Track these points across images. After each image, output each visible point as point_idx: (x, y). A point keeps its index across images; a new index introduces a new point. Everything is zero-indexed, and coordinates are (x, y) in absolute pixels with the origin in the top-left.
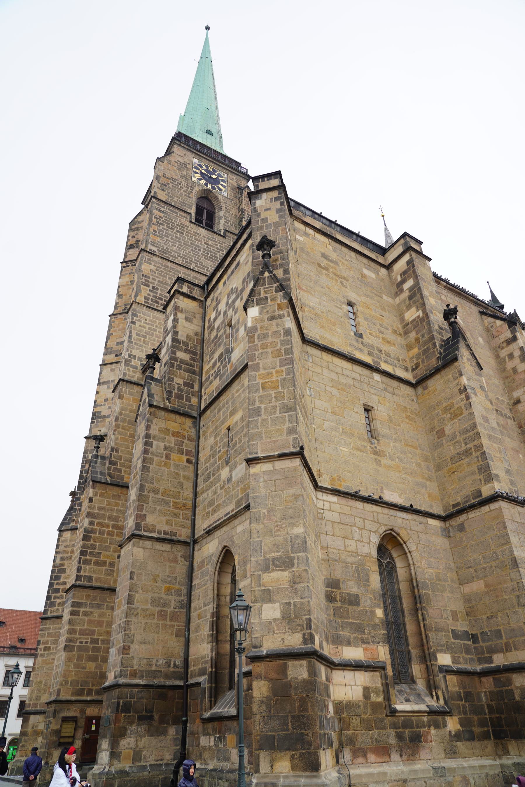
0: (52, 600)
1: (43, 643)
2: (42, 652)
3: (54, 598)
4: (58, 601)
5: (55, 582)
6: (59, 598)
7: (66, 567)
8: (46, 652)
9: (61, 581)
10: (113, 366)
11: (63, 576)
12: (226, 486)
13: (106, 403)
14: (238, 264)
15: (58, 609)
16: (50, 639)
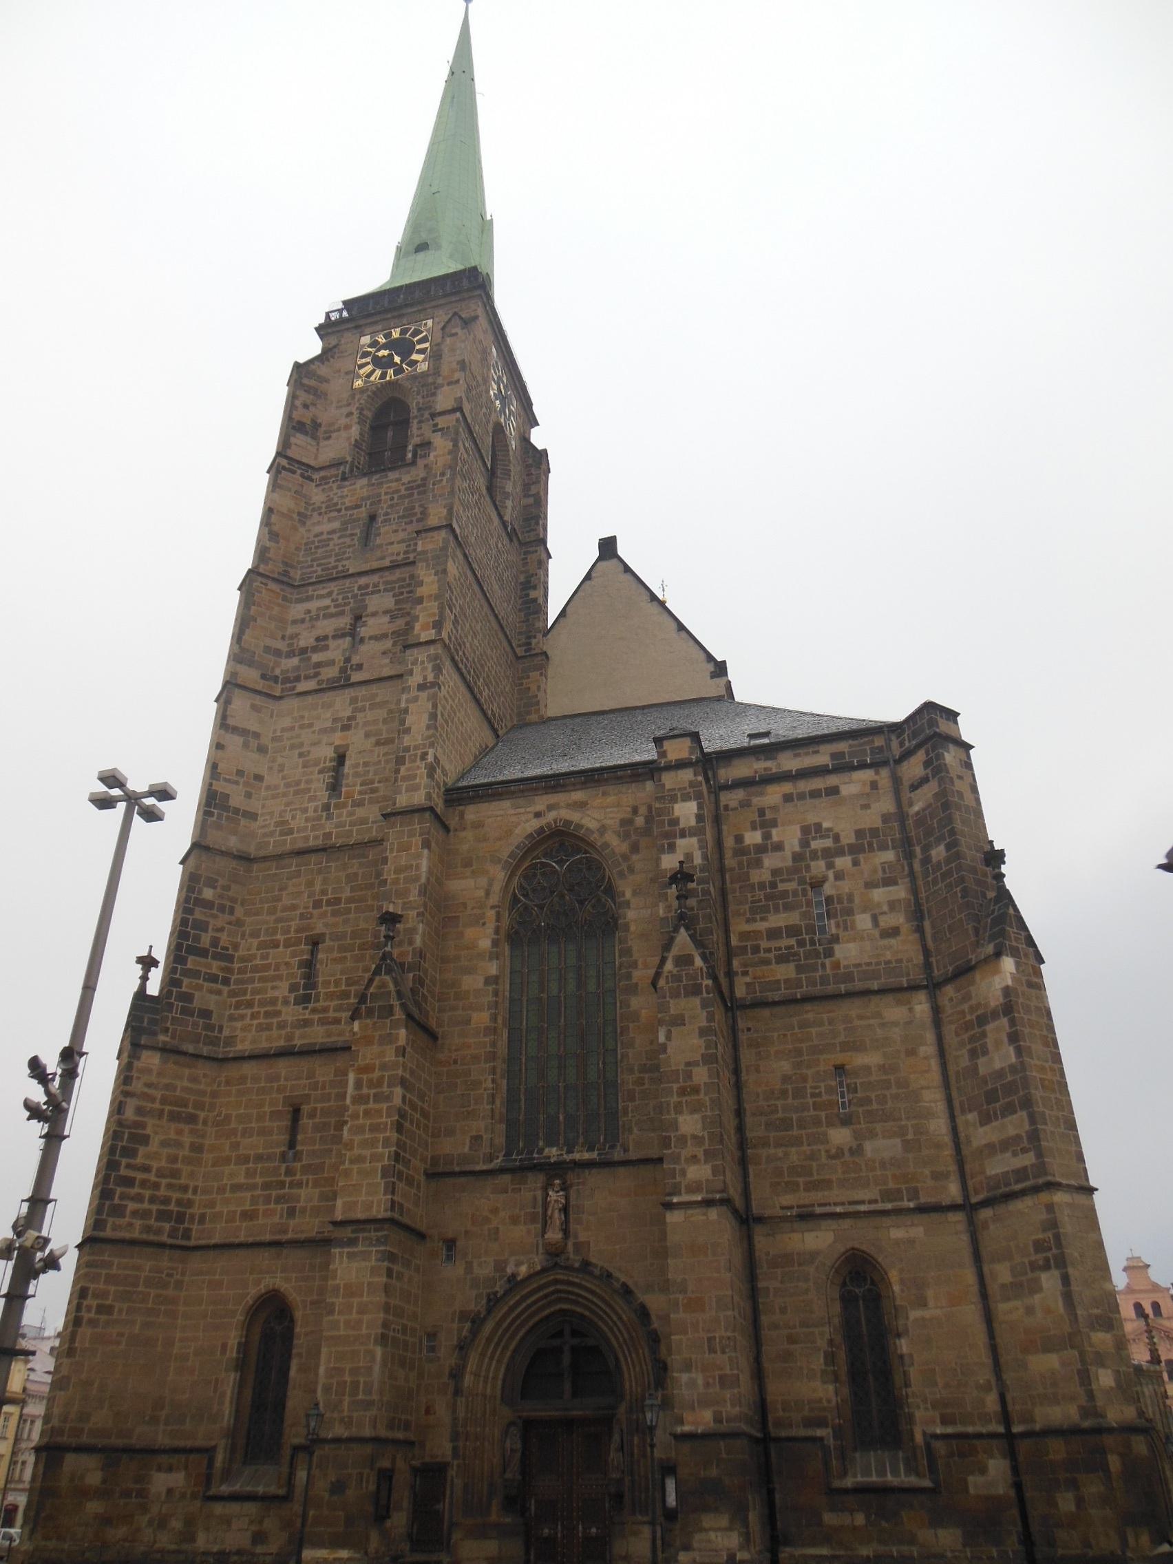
0: (116, 1201)
1: (96, 1296)
2: (92, 1315)
3: (121, 1198)
4: (132, 1206)
5: (124, 1161)
6: (132, 1199)
7: (149, 1131)
8: (103, 1318)
9: (139, 1160)
10: (258, 700)
11: (142, 1150)
12: (847, 1157)
13: (241, 781)
14: (834, 791)
15: (131, 1225)
16: (112, 1288)
